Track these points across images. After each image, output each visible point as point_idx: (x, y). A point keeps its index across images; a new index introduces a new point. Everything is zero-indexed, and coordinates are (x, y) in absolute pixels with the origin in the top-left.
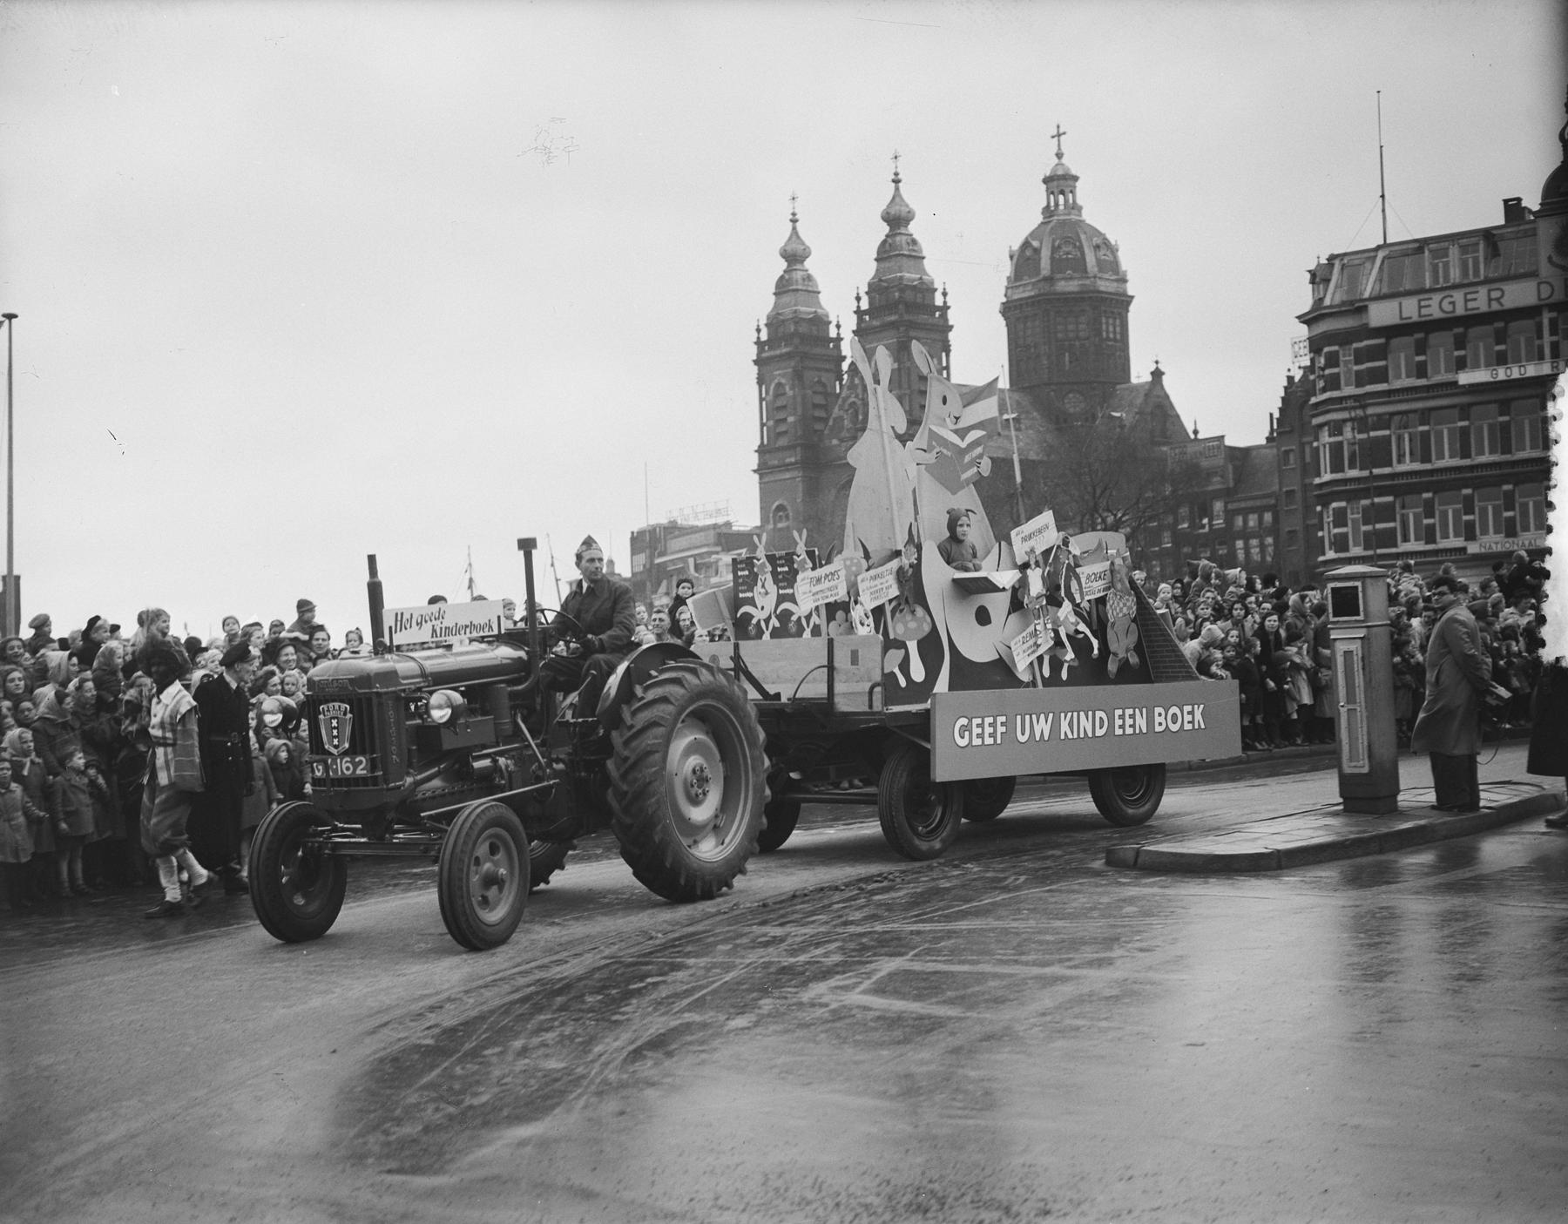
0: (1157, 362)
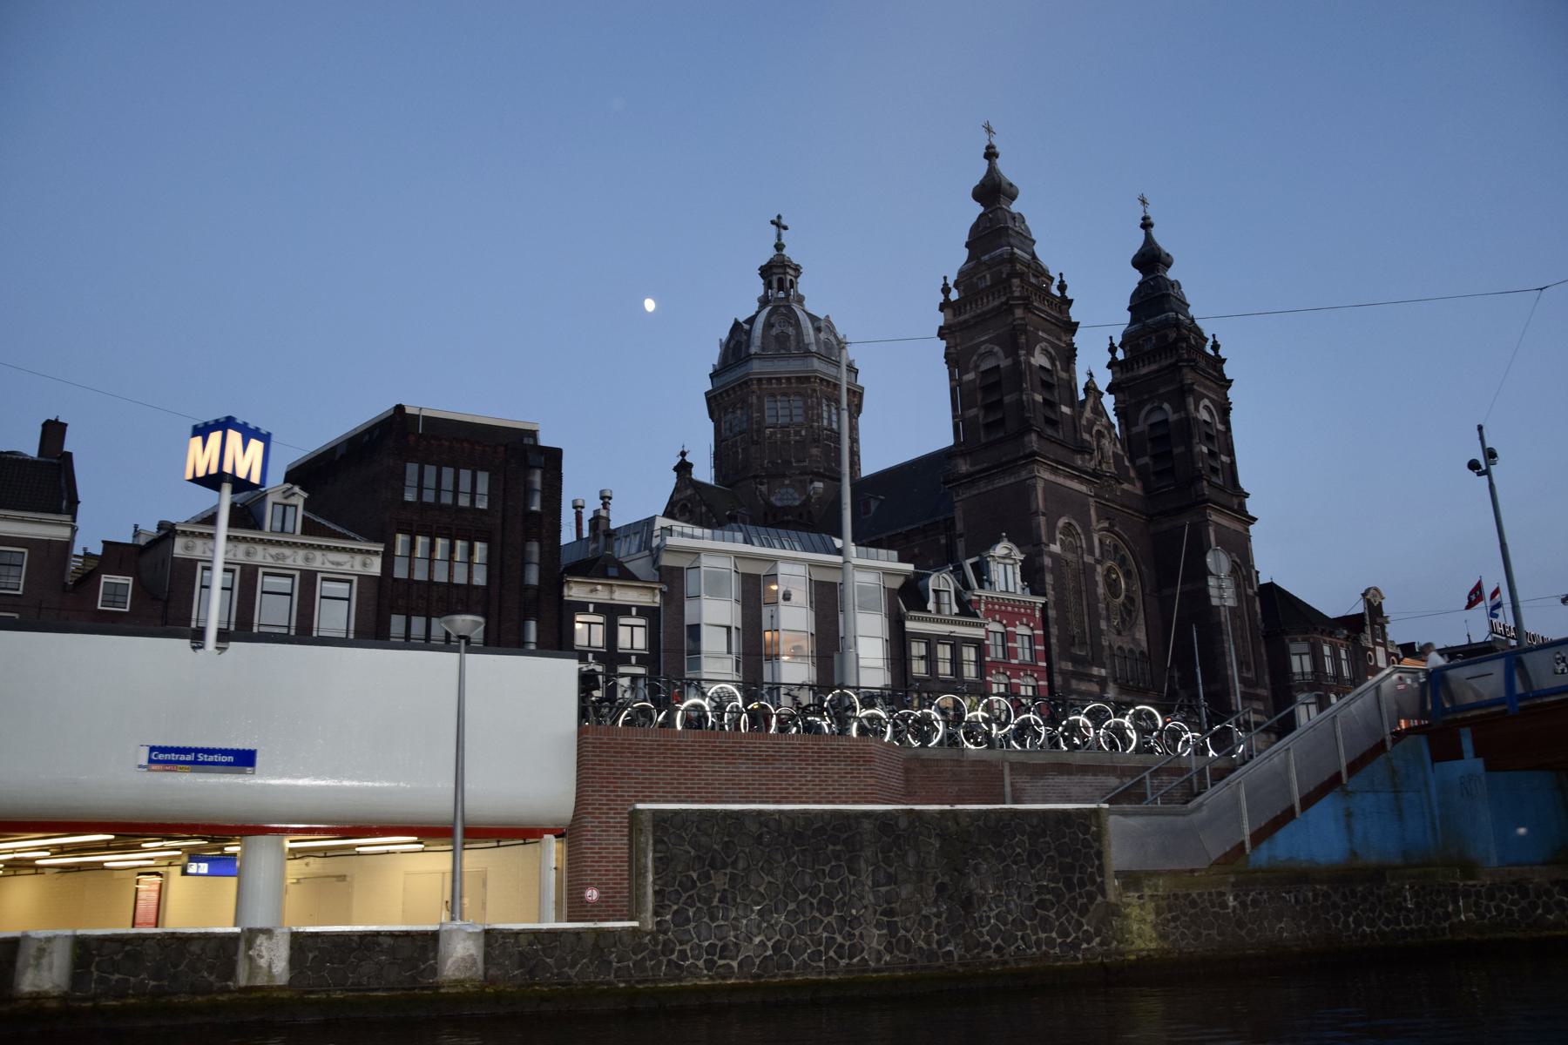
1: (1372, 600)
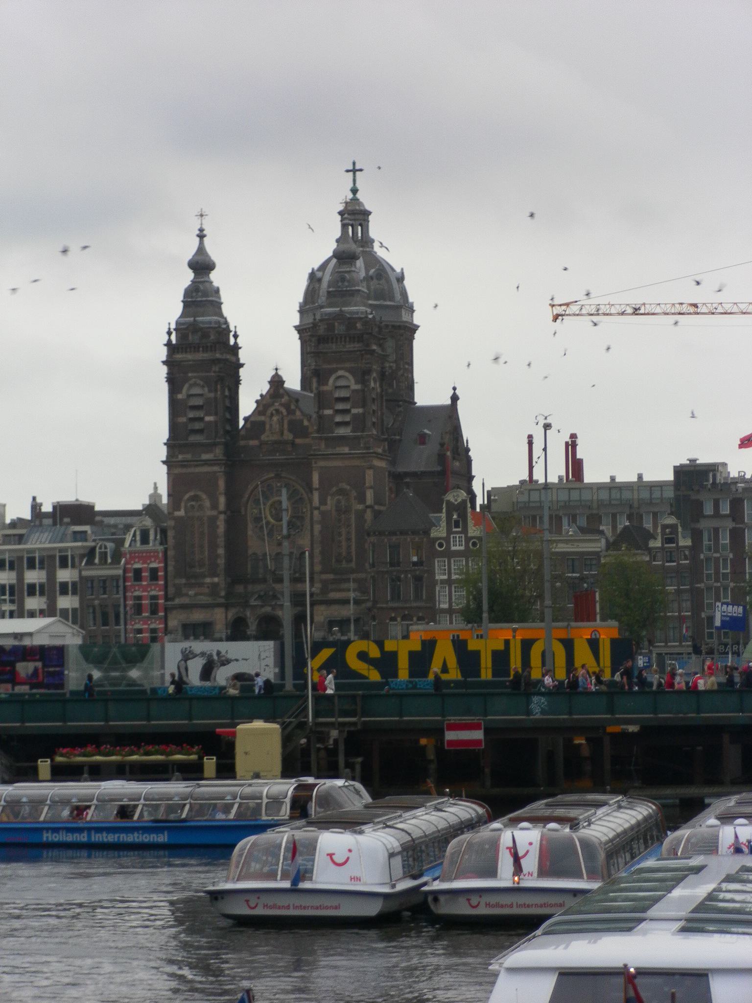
0: (454, 389)
1: (452, 500)
